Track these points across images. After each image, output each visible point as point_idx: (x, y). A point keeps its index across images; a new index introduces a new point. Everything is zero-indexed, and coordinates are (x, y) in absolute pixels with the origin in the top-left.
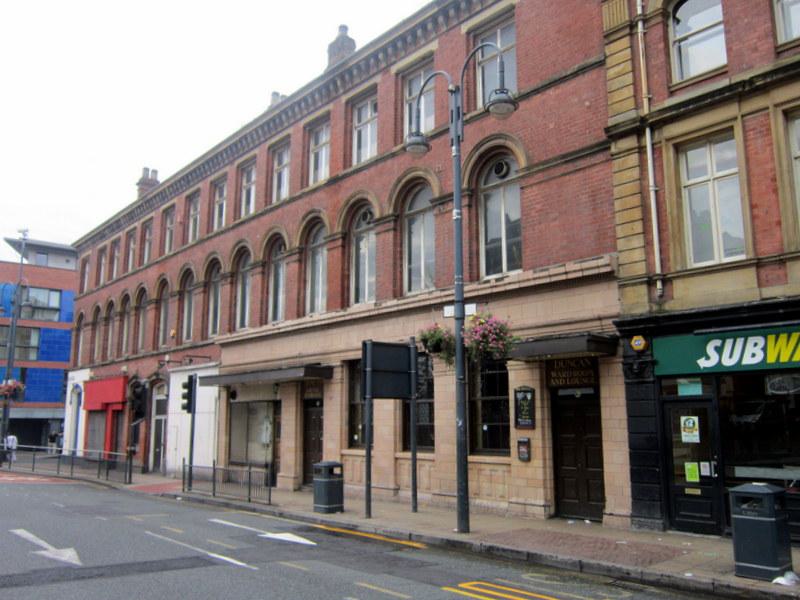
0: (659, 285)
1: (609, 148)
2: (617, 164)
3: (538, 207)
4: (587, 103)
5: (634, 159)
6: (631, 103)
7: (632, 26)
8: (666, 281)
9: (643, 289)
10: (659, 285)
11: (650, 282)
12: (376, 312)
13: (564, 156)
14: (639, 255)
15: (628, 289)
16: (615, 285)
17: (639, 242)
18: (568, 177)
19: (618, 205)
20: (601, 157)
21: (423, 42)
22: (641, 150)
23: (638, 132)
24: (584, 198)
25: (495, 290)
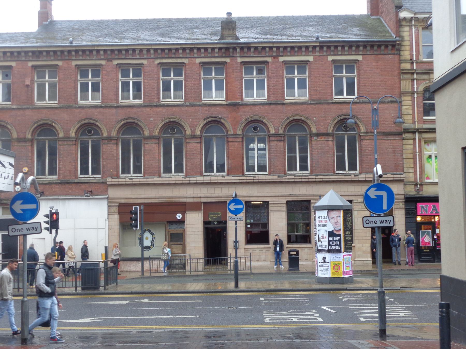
0: (419, 186)
1: (402, 135)
2: (405, 142)
3: (370, 149)
4: (393, 115)
5: (411, 142)
6: (411, 121)
7: (413, 93)
8: (421, 185)
9: (413, 186)
10: (419, 186)
11: (416, 185)
12: (279, 180)
13: (383, 133)
14: (411, 175)
15: (407, 186)
16: (403, 183)
17: (411, 170)
18: (383, 141)
19: (405, 156)
20: (397, 137)
21: (303, 54)
22: (414, 139)
23: (414, 133)
24: (390, 150)
25: (353, 179)
